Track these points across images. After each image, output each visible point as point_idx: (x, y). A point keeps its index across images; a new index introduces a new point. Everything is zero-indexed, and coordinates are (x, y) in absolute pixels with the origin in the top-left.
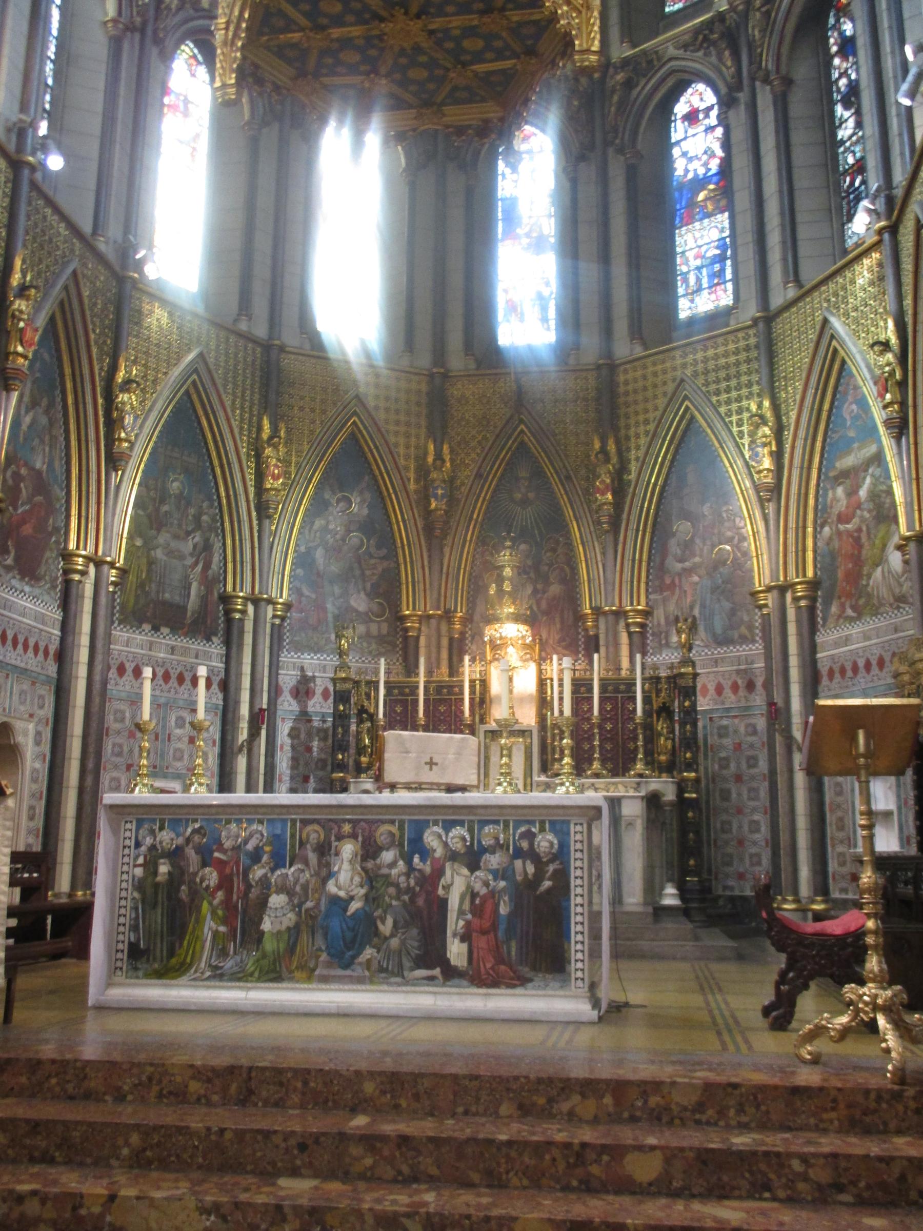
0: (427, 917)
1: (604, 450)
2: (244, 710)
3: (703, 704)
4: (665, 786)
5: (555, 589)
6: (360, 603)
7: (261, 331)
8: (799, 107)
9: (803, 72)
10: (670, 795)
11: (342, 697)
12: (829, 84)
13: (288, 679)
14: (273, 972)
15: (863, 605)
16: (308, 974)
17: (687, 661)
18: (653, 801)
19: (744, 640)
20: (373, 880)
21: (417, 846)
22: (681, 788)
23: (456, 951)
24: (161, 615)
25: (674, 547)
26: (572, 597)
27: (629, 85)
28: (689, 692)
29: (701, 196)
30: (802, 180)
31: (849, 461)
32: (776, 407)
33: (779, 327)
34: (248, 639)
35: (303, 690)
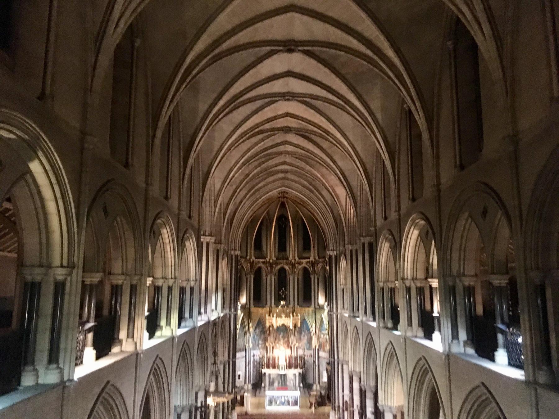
4: (301, 371)
6: (260, 342)
10: (301, 373)
13: (252, 354)
14: (279, 405)
18: (300, 374)
25: (302, 335)
26: (288, 341)
35: (254, 356)
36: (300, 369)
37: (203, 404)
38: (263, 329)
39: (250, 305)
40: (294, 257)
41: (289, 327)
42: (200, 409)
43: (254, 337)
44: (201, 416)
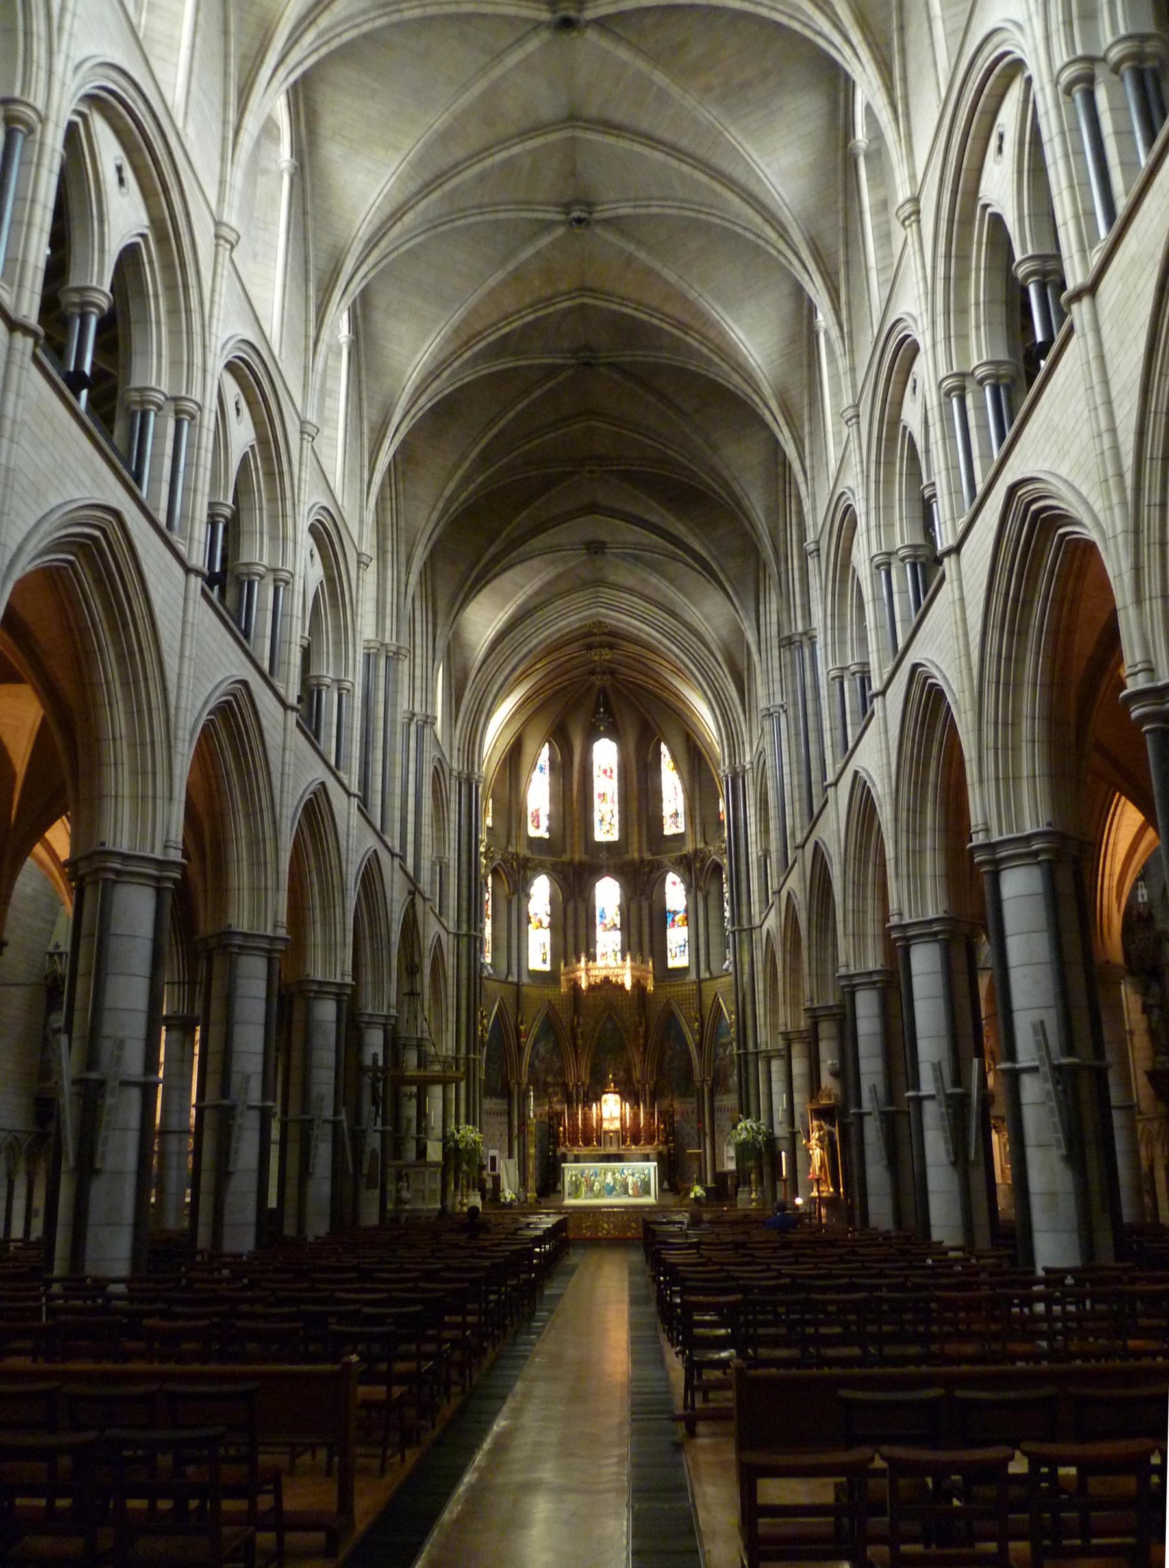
0: (625, 1186)
1: (641, 1022)
2: (516, 1123)
3: (676, 1118)
5: (622, 1073)
7: (515, 979)
8: (712, 902)
9: (713, 888)
10: (665, 1152)
11: (551, 1119)
12: (722, 894)
14: (597, 1197)
15: (727, 1091)
16: (602, 1197)
17: (672, 1106)
19: (691, 1096)
20: (614, 1179)
21: (623, 1172)
22: (669, 1150)
23: (631, 1192)
24: (490, 1092)
27: (650, 872)
28: (672, 1116)
29: (677, 918)
30: (712, 930)
31: (723, 1040)
32: (701, 1015)
33: (703, 985)
34: (516, 1097)
36: (666, 1142)
37: (380, 1063)
38: (557, 1042)
39: (519, 975)
40: (640, 851)
41: (623, 985)
42: (370, 1074)
43: (531, 1065)
44: (375, 1090)
